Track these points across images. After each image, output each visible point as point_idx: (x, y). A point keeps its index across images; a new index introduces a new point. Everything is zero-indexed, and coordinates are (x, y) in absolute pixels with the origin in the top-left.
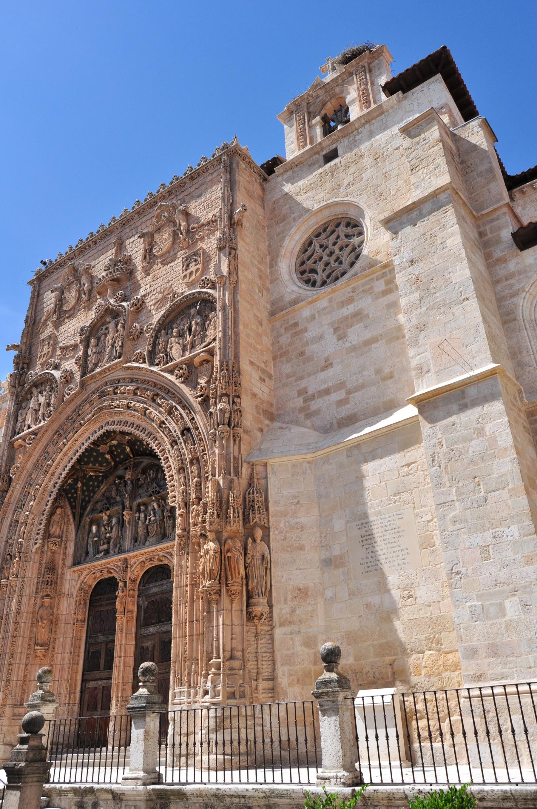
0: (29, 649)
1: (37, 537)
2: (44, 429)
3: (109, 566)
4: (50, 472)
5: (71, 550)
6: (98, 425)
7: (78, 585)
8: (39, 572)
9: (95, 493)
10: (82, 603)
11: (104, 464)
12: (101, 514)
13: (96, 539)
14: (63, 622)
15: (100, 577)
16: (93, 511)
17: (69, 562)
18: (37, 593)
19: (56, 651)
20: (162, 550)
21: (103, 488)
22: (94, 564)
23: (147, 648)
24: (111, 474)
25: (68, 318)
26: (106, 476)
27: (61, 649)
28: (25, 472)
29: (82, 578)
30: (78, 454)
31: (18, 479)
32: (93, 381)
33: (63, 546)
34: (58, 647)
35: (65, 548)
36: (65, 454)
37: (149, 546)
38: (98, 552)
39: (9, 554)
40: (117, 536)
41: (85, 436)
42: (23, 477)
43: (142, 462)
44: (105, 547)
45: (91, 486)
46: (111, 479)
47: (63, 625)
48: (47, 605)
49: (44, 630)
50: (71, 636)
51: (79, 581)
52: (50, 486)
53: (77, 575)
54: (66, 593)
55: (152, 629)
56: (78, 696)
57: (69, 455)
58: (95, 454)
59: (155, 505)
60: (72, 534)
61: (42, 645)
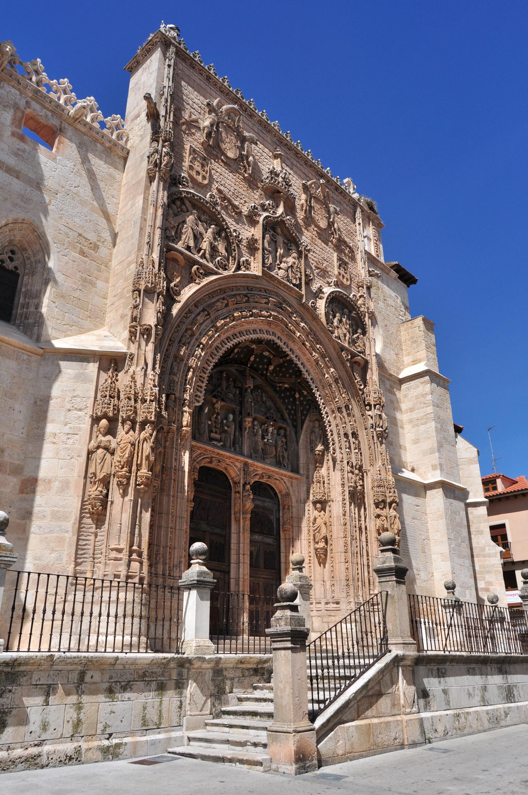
12: (214, 400)
25: (222, 161)
32: (268, 279)
37: (271, 464)
44: (218, 436)
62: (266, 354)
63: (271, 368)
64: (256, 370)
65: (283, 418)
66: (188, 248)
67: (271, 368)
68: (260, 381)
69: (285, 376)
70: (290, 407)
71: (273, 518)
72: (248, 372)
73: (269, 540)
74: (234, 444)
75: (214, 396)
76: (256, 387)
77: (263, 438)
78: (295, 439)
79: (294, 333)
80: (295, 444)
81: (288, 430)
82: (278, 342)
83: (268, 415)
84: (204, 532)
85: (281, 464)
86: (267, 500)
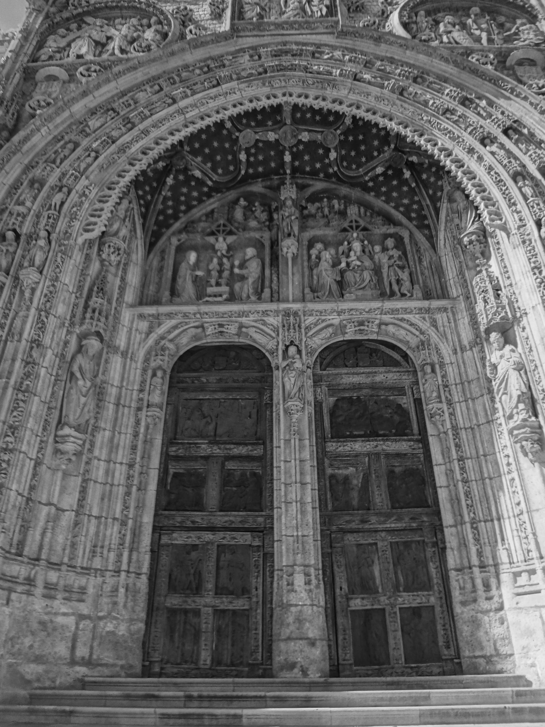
0: (45, 429)
1: (93, 219)
2: (130, 64)
3: (244, 320)
4: (141, 127)
5: (134, 277)
7: (151, 341)
8: (80, 288)
9: (190, 208)
10: (159, 373)
11: (220, 171)
13: (200, 273)
14: (112, 400)
17: (130, 296)
18: (72, 324)
19: (96, 453)
20: (393, 311)
21: (213, 204)
23: (346, 479)
26: (217, 188)
27: (105, 451)
28: (66, 114)
29: (161, 331)
30: (191, 129)
31: (50, 119)
32: (255, 33)
33: (122, 266)
34: (101, 448)
35: (125, 271)
37: (358, 299)
39: (14, 230)
42: (58, 120)
43: (308, 186)
45: (183, 194)
46: (231, 195)
47: (111, 406)
48: (91, 352)
49: (83, 400)
50: (130, 430)
51: (153, 337)
52: (133, 149)
53: (144, 325)
54: (122, 348)
56: (146, 559)
57: (188, 116)
58: (216, 144)
59: (357, 246)
60: (138, 255)
61: (78, 429)
62: (305, 137)
66: (79, 57)
67: (333, 155)
69: (373, 158)
70: (406, 201)
71: (407, 402)
73: (402, 446)
75: (212, 234)
78: (427, 245)
79: (331, 74)
80: (431, 251)
81: (406, 235)
84: (206, 458)
86: (382, 369)
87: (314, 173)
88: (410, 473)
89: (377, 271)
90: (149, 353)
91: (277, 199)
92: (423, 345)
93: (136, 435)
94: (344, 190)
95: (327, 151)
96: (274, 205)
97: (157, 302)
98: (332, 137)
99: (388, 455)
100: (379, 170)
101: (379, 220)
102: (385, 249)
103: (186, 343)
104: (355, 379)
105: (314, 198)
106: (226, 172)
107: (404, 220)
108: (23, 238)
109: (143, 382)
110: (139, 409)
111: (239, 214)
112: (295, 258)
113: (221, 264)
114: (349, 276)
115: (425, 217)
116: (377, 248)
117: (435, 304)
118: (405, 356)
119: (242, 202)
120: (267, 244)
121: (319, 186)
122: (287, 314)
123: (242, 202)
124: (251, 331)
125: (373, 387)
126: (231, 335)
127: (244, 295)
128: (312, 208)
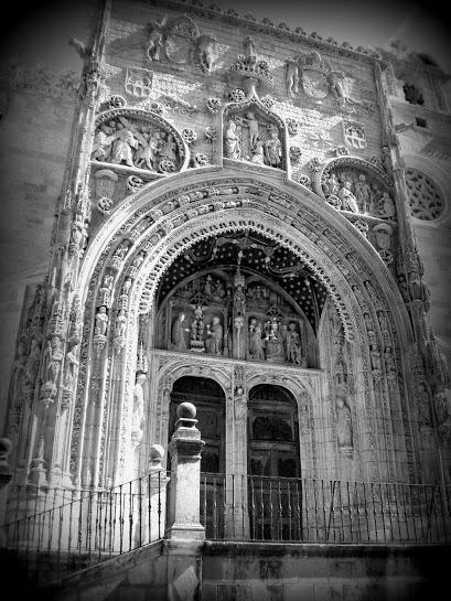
6: (240, 218)
7: (162, 373)
9: (180, 280)
12: (194, 307)
13: (187, 330)
15: (195, 373)
16: (174, 295)
21: (192, 277)
22: (193, 357)
23: (259, 462)
24: (203, 268)
26: (196, 267)
36: (190, 226)
38: (190, 347)
40: (223, 340)
41: (222, 220)
44: (201, 343)
46: (204, 273)
55: (265, 445)
62: (254, 246)
63: (268, 260)
64: (253, 266)
65: (294, 311)
66: (124, 162)
67: (268, 260)
68: (256, 277)
70: (304, 298)
71: (290, 423)
72: (238, 270)
74: (222, 348)
75: (193, 303)
76: (252, 285)
77: (264, 336)
81: (301, 322)
82: (259, 230)
83: (270, 310)
85: (291, 360)
87: (253, 266)
88: (290, 461)
89: (284, 343)
90: (161, 379)
91: (233, 283)
92: (304, 394)
93: (158, 429)
94: (269, 283)
95: (264, 256)
96: (229, 285)
97: (164, 348)
98: (270, 252)
99: (280, 451)
100: (292, 275)
101: (288, 309)
102: (289, 330)
103: (180, 375)
104: (265, 407)
105: (252, 285)
106: (202, 255)
107: (302, 312)
108: (110, 312)
109: (159, 398)
110: (159, 415)
111: (208, 288)
112: (242, 328)
113: (198, 324)
114: (270, 345)
115: (312, 311)
116: (285, 327)
117: (314, 372)
118: (292, 396)
119: (209, 278)
120: (226, 315)
121: (256, 277)
122: (237, 367)
123: (209, 278)
124: (216, 374)
125: (275, 412)
126: (206, 374)
127: (213, 350)
128: (251, 292)
